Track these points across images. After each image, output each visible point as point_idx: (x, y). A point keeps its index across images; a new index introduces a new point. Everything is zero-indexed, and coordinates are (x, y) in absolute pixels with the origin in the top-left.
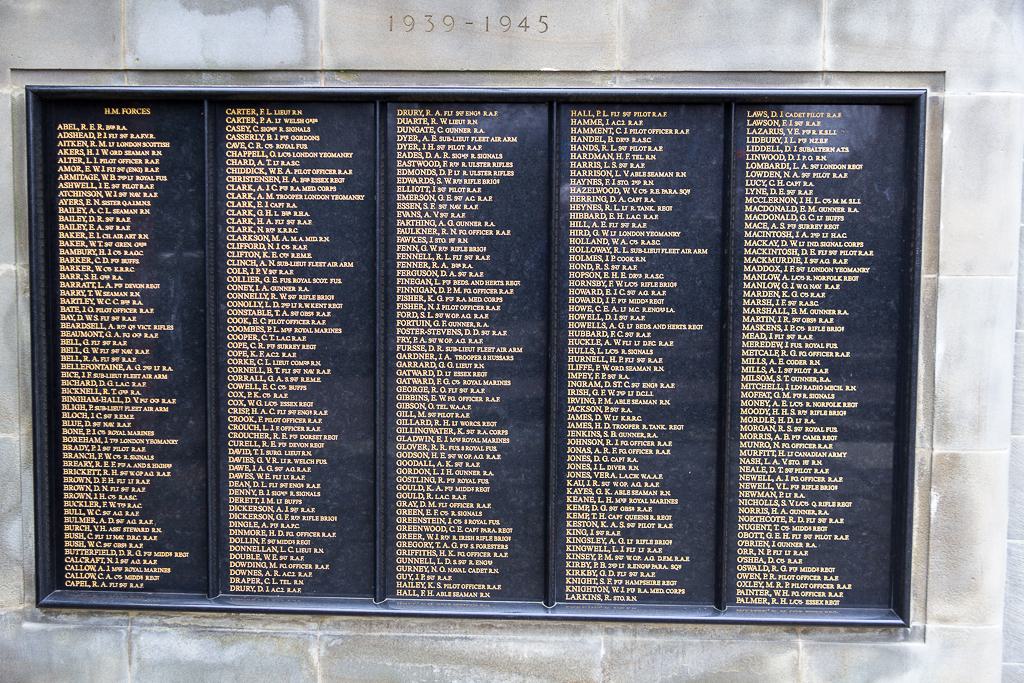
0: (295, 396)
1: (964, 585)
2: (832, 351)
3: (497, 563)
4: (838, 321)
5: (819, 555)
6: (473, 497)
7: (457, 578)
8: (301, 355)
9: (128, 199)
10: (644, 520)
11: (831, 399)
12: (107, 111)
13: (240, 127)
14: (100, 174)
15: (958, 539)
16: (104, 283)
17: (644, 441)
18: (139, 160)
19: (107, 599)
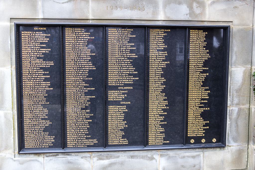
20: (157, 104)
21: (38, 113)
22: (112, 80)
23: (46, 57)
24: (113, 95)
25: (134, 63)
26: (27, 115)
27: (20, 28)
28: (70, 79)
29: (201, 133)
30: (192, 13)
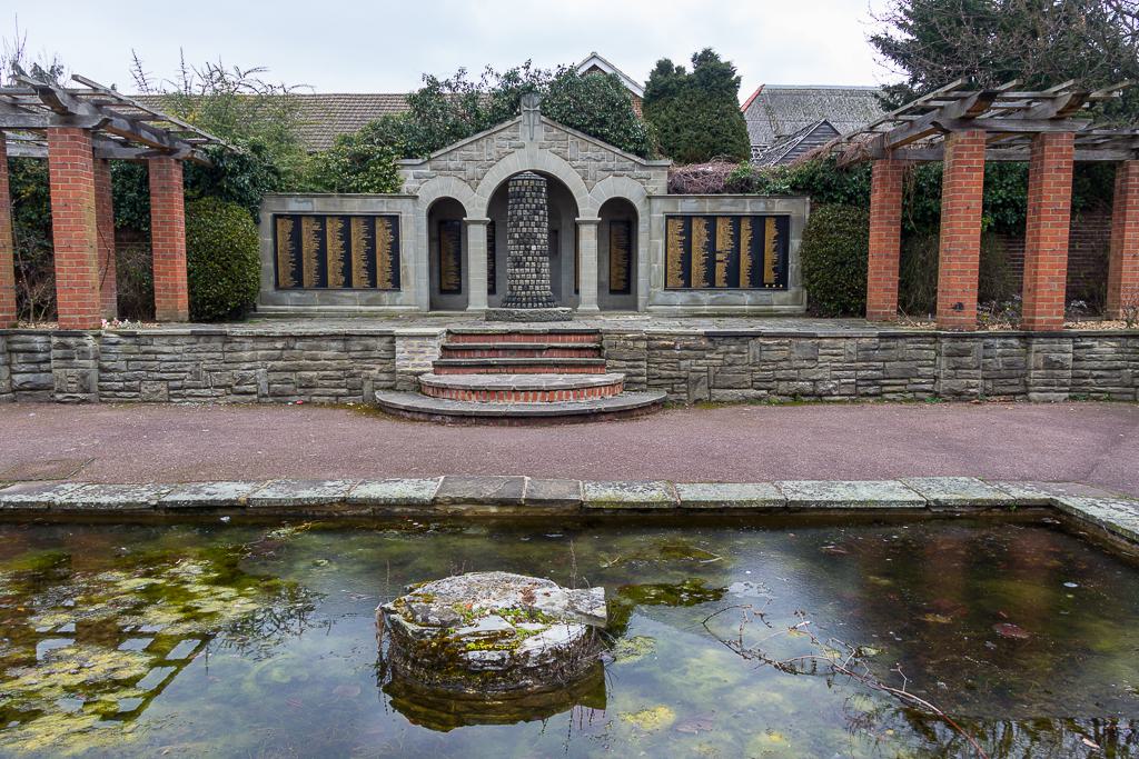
1: (408, 284)
5: (389, 280)
11: (389, 258)
13: (304, 220)
15: (407, 277)
17: (363, 264)
18: (289, 223)
19: (285, 289)
20: (745, 262)
21: (676, 268)
22: (718, 248)
23: (681, 234)
24: (718, 257)
25: (732, 237)
26: (669, 267)
27: (668, 217)
28: (694, 247)
29: (773, 281)
30: (766, 208)
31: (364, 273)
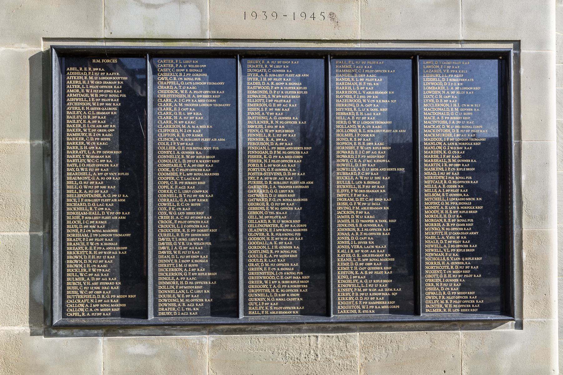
0: (194, 209)
2: (469, 180)
3: (302, 295)
4: (471, 165)
6: (288, 260)
7: (281, 304)
8: (197, 187)
9: (104, 106)
10: (378, 270)
12: (94, 61)
14: (89, 94)
16: (91, 151)
31: (379, 260)
